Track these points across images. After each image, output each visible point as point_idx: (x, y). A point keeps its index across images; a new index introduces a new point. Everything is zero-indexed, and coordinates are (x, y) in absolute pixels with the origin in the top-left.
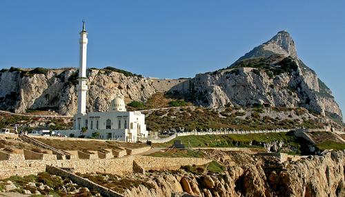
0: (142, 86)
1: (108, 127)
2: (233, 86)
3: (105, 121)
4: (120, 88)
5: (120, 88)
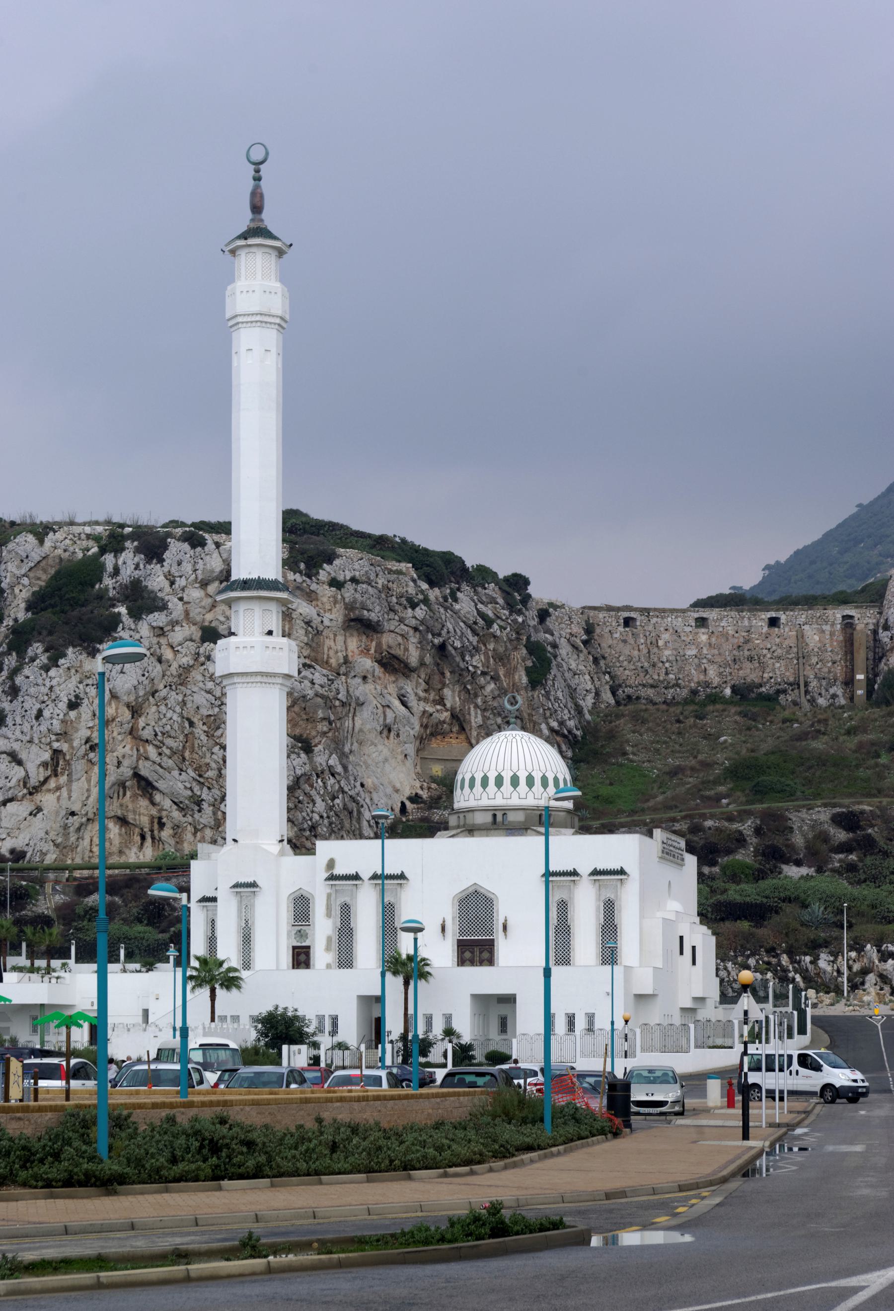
0: (534, 649)
1: (476, 950)
3: (448, 912)
4: (392, 664)
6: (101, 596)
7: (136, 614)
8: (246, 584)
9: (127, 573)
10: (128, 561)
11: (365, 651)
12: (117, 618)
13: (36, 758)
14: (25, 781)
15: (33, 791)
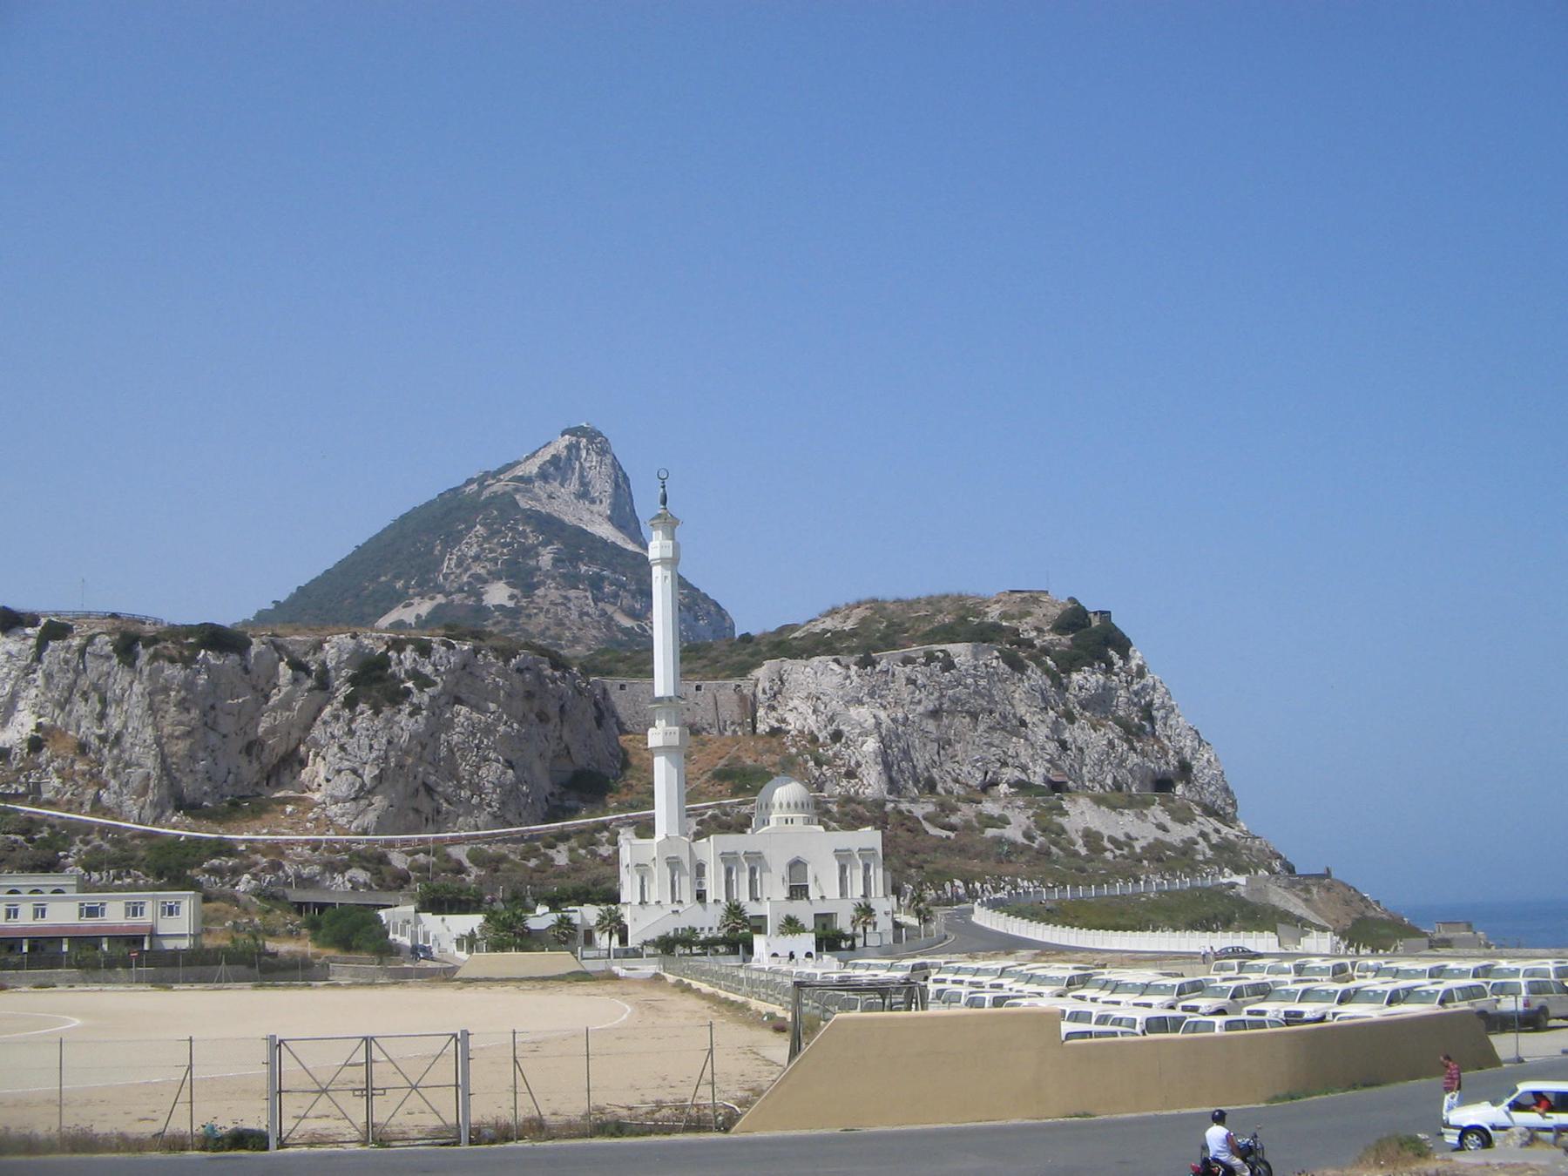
1: (798, 891)
2: (935, 714)
3: (784, 870)
5: (543, 718)
6: (393, 676)
7: (421, 690)
8: (660, 700)
9: (408, 664)
10: (409, 655)
11: (531, 710)
12: (408, 692)
13: (369, 773)
14: (363, 785)
15: (369, 792)
